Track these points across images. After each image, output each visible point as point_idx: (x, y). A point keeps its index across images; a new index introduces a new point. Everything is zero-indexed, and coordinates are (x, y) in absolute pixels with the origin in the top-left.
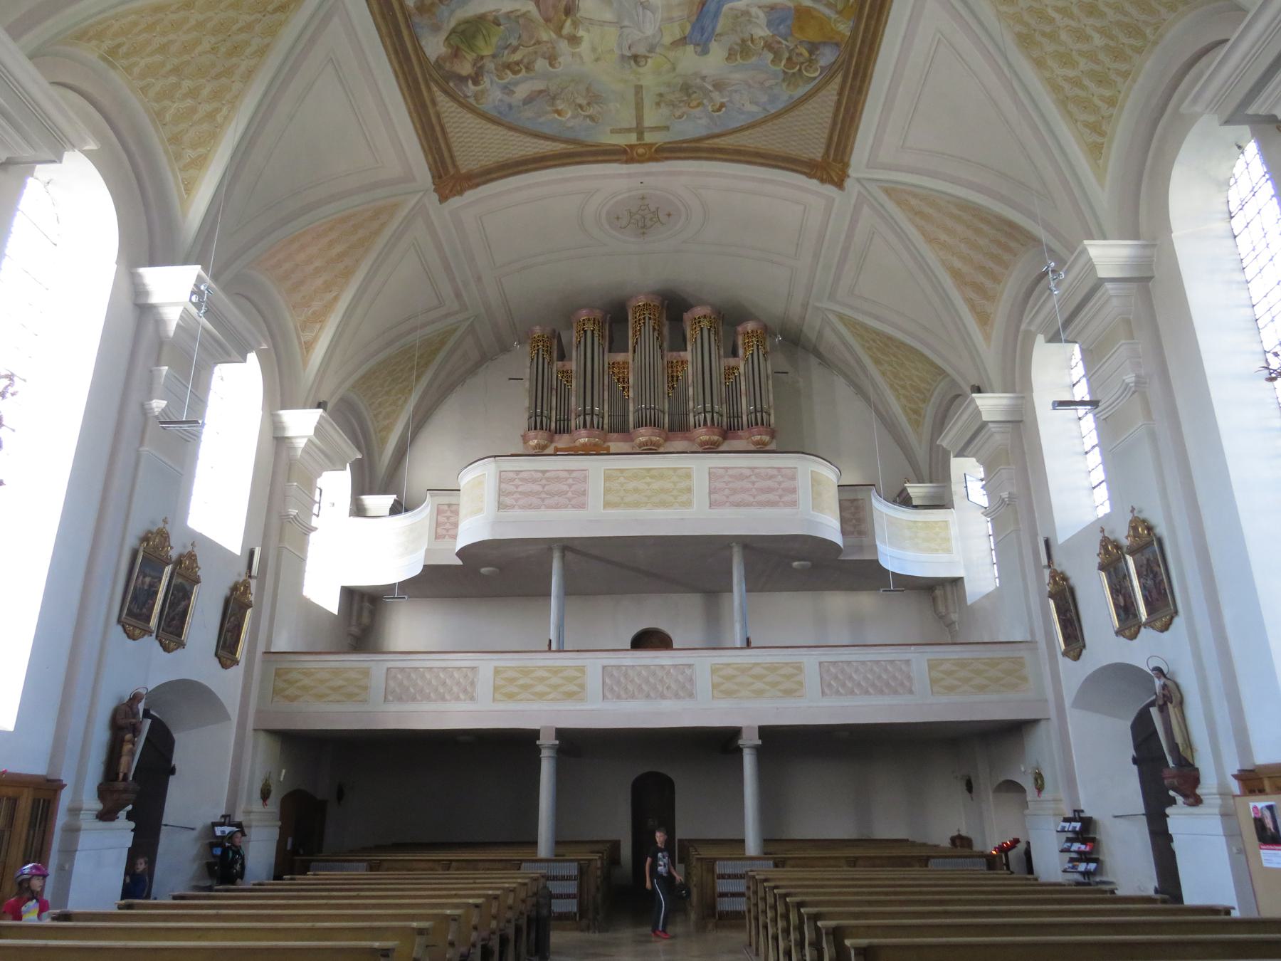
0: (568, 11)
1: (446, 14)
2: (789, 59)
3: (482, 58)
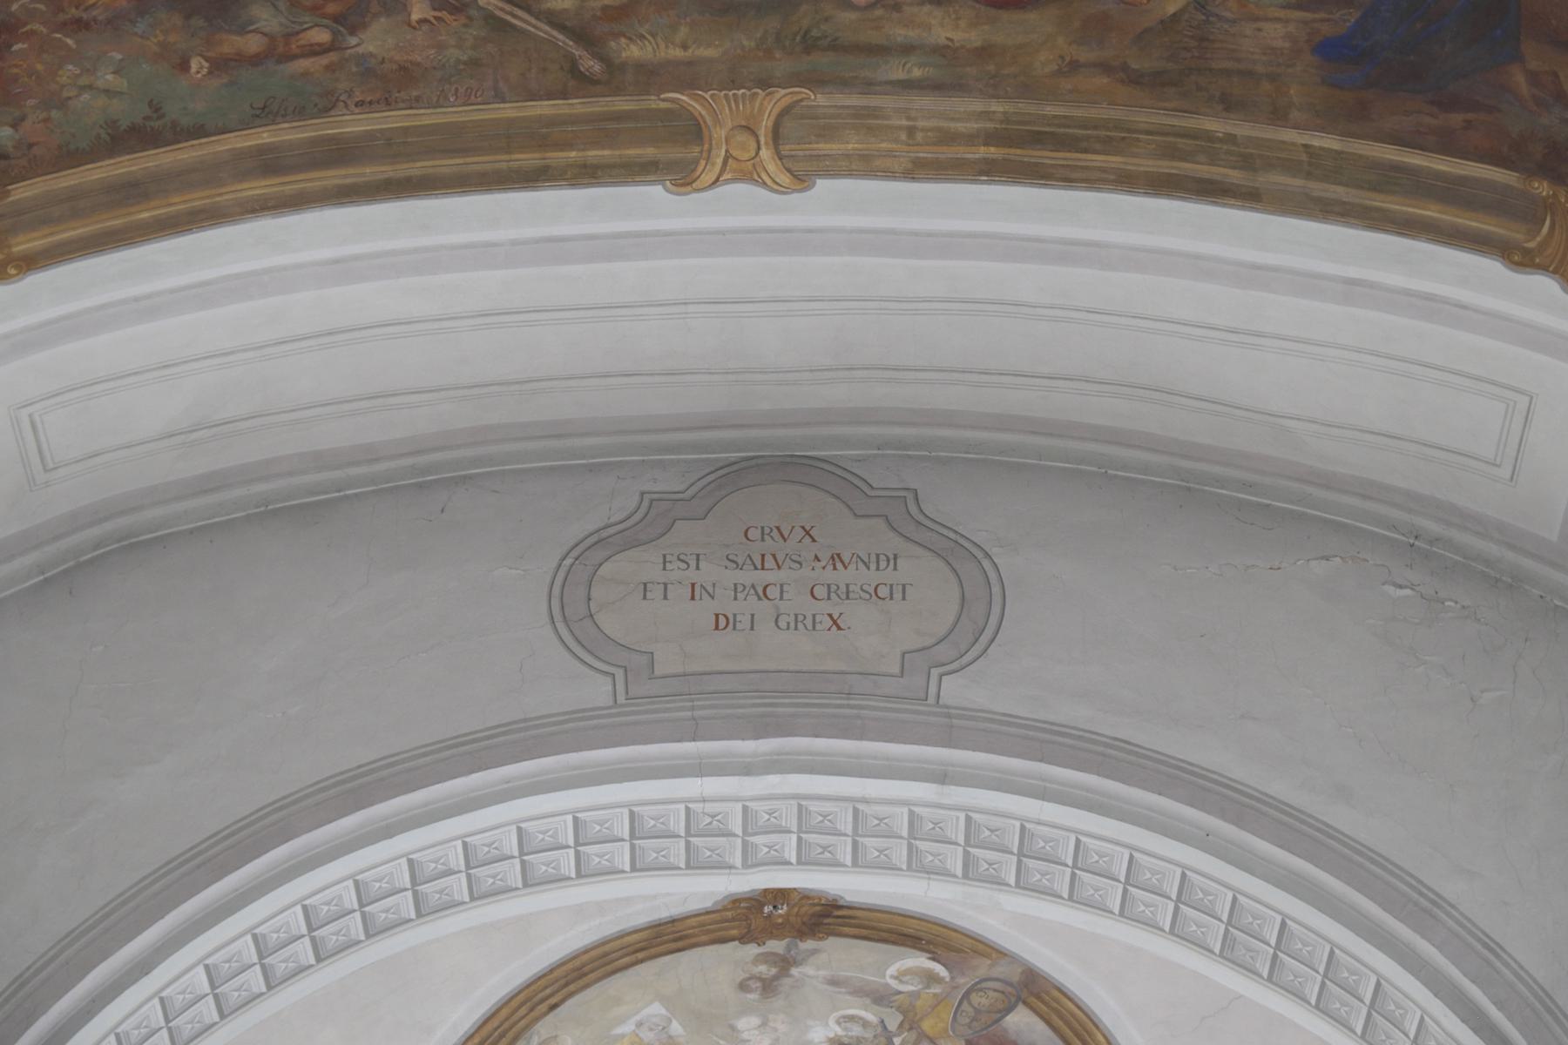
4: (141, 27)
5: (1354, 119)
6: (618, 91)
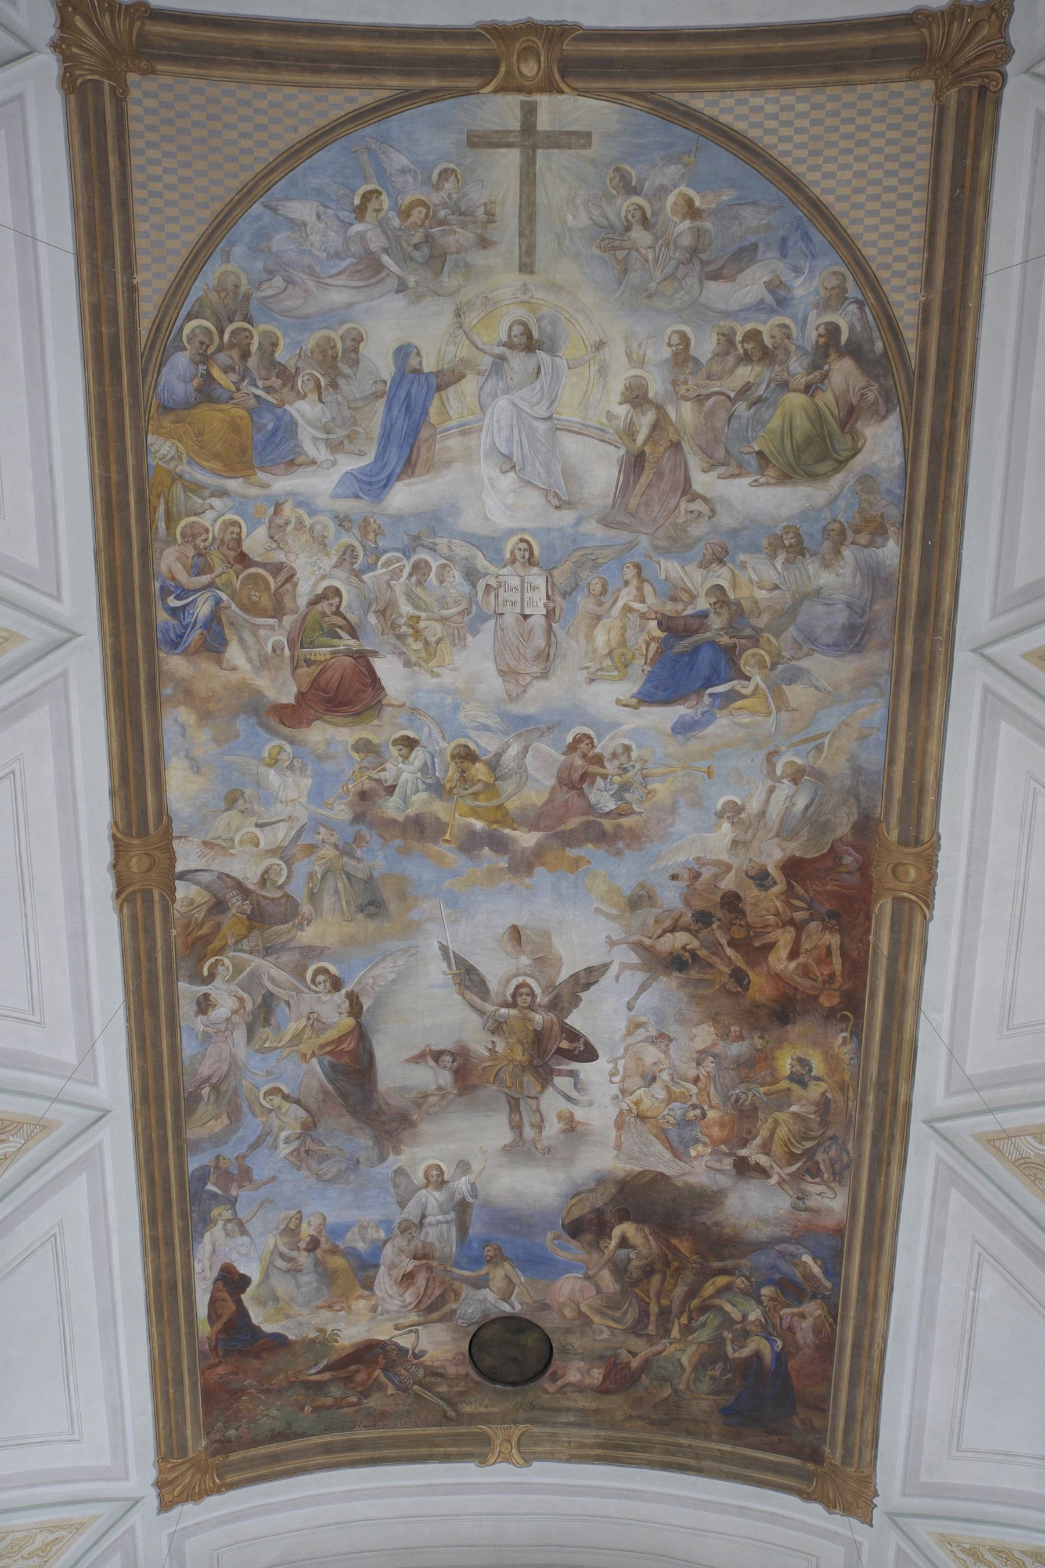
0: (635, 463)
1: (841, 504)
2: (245, 355)
3: (808, 389)
4: (290, 1393)
5: (735, 1438)
6: (461, 1424)
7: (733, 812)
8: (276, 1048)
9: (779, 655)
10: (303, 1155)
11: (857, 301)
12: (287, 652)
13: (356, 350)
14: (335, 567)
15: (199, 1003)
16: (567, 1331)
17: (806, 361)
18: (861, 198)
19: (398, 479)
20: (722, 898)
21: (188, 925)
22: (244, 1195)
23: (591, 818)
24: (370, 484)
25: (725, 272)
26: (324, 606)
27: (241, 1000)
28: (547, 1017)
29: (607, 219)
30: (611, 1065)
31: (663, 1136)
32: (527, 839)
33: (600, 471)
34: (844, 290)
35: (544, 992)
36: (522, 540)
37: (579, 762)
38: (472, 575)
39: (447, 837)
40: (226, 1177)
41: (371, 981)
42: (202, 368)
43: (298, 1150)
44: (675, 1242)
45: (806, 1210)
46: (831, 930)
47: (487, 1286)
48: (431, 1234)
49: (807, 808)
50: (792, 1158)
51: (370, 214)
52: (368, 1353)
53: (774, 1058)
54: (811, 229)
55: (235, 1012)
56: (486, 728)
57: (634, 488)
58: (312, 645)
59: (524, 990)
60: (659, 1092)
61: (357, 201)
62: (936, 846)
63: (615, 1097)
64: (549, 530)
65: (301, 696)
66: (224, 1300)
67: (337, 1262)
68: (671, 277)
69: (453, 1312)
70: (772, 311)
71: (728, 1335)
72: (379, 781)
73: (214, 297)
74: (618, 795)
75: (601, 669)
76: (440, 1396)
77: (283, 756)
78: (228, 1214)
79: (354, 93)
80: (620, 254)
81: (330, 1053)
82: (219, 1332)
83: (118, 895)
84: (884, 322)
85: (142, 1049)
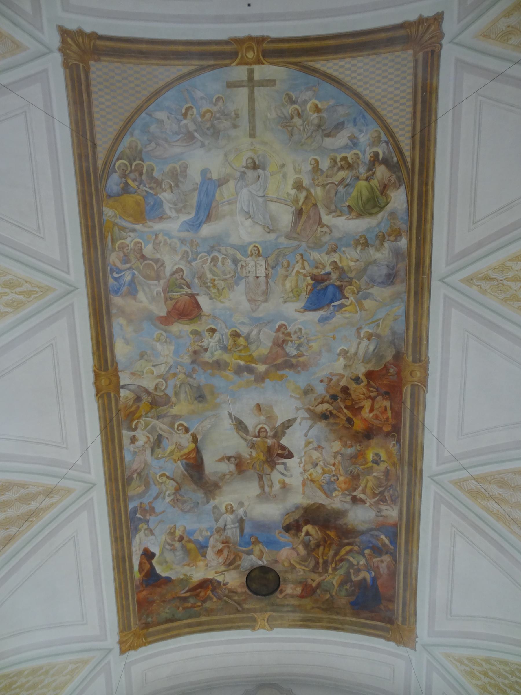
0: (299, 213)
1: (383, 225)
2: (141, 174)
3: (367, 179)
5: (356, 614)
7: (344, 353)
8: (163, 457)
9: (360, 288)
10: (176, 501)
11: (385, 142)
12: (162, 295)
13: (185, 171)
14: (180, 260)
15: (131, 439)
16: (286, 572)
17: (366, 168)
18: (385, 100)
19: (205, 223)
20: (341, 389)
21: (126, 407)
22: (152, 519)
23: (287, 358)
24: (193, 225)
25: (332, 133)
26: (177, 276)
27: (148, 437)
28: (272, 441)
29: (284, 114)
30: (300, 460)
31: (321, 488)
32: (261, 368)
33: (285, 217)
34: (380, 138)
35: (271, 430)
36: (255, 246)
37: (281, 335)
38: (235, 261)
39: (229, 368)
40: (144, 511)
41: (201, 429)
42: (124, 180)
43: (173, 499)
44: (328, 532)
45: (381, 516)
46: (386, 400)
47: (252, 554)
48: (229, 533)
49: (374, 350)
50: (375, 495)
51: (189, 116)
52: (204, 584)
53: (365, 454)
54: (366, 114)
55: (146, 443)
56: (243, 323)
57: (299, 223)
58: (172, 291)
59: (263, 430)
60: (319, 470)
61: (183, 111)
62: (427, 362)
63: (301, 473)
64: (266, 242)
65: (169, 313)
66: (145, 563)
67: (191, 546)
68: (311, 136)
69: (239, 565)
70: (351, 148)
71: (352, 571)
72: (201, 346)
73: (128, 151)
74: (297, 348)
75: (289, 298)
76: (235, 601)
77: (162, 337)
78: (145, 527)
79: (180, 67)
80: (290, 129)
81: (186, 458)
82: (144, 576)
83: (97, 395)
84: (397, 149)
85: (108, 458)
